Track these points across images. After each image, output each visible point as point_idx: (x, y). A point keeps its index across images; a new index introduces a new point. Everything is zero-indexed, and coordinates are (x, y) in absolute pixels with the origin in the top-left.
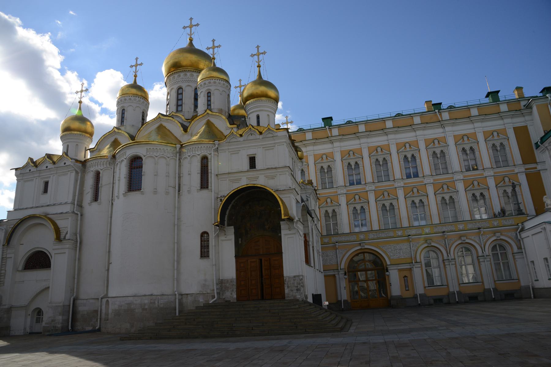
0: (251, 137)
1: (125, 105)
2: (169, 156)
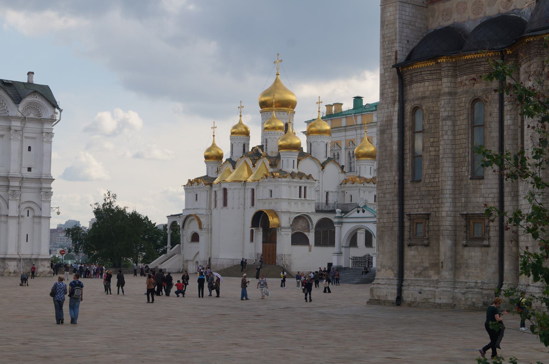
0: (271, 180)
1: (233, 142)
2: (239, 188)
